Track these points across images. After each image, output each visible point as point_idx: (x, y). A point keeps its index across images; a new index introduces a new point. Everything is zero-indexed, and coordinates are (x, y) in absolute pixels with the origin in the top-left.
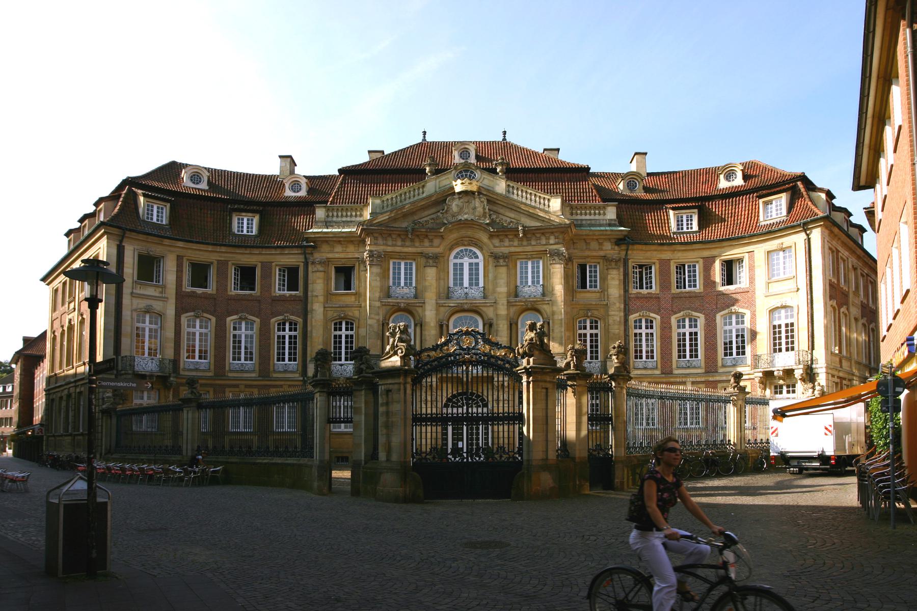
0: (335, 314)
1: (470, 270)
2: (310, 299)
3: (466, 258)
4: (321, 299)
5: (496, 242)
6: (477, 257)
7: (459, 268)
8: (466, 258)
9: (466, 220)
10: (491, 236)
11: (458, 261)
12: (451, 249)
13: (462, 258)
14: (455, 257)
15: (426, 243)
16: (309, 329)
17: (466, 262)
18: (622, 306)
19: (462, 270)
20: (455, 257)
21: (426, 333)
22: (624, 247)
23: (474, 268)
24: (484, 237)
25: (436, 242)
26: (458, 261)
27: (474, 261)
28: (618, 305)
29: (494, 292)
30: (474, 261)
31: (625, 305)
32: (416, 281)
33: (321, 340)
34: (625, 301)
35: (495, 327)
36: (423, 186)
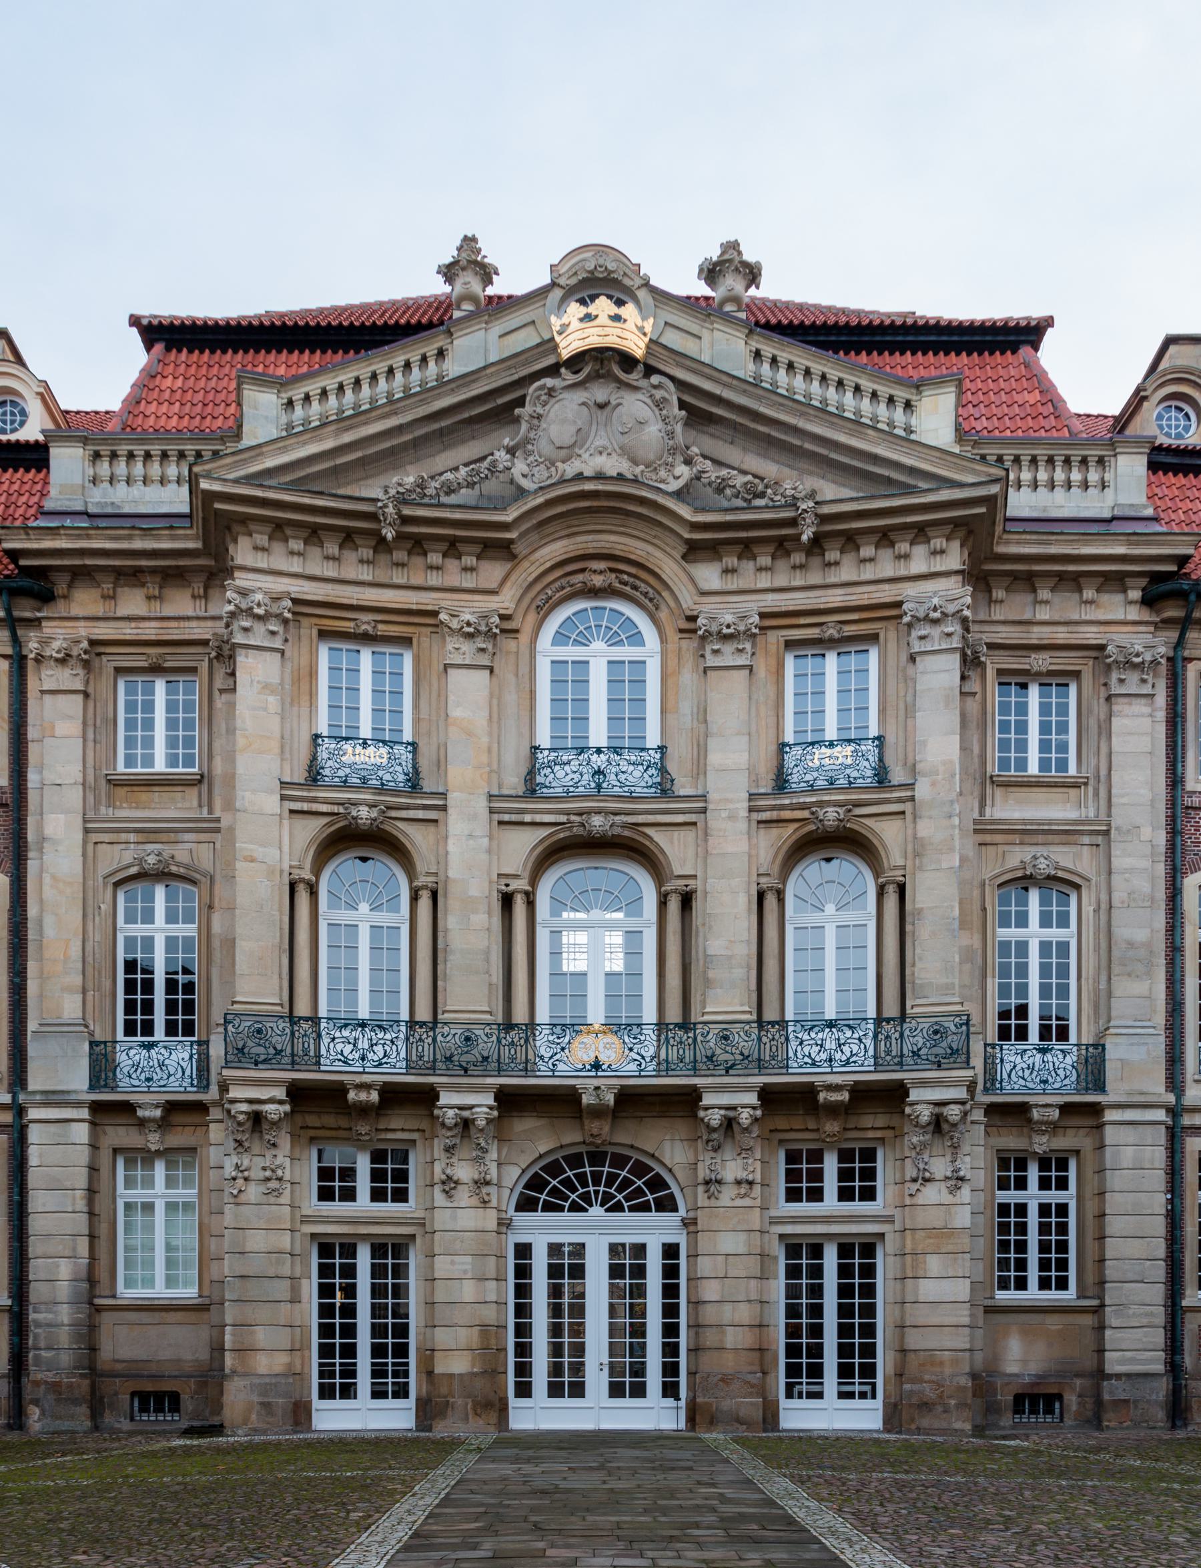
0: (128, 857)
1: (614, 682)
2: (32, 797)
3: (598, 645)
4: (74, 797)
5: (709, 575)
6: (636, 639)
7: (572, 678)
8: (598, 645)
9: (600, 477)
10: (694, 551)
11: (570, 652)
12: (545, 609)
13: (582, 641)
14: (561, 638)
15: (453, 575)
16: (32, 911)
17: (599, 656)
18: (1161, 838)
19: (583, 682)
20: (561, 638)
21: (451, 922)
22: (1174, 612)
23: (626, 679)
24: (669, 566)
25: (492, 572)
26: (570, 652)
27: (627, 652)
28: (1146, 833)
29: (700, 768)
30: (627, 652)
31: (1174, 831)
32: (417, 721)
33: (75, 950)
34: (1172, 820)
35: (697, 905)
36: (441, 354)
